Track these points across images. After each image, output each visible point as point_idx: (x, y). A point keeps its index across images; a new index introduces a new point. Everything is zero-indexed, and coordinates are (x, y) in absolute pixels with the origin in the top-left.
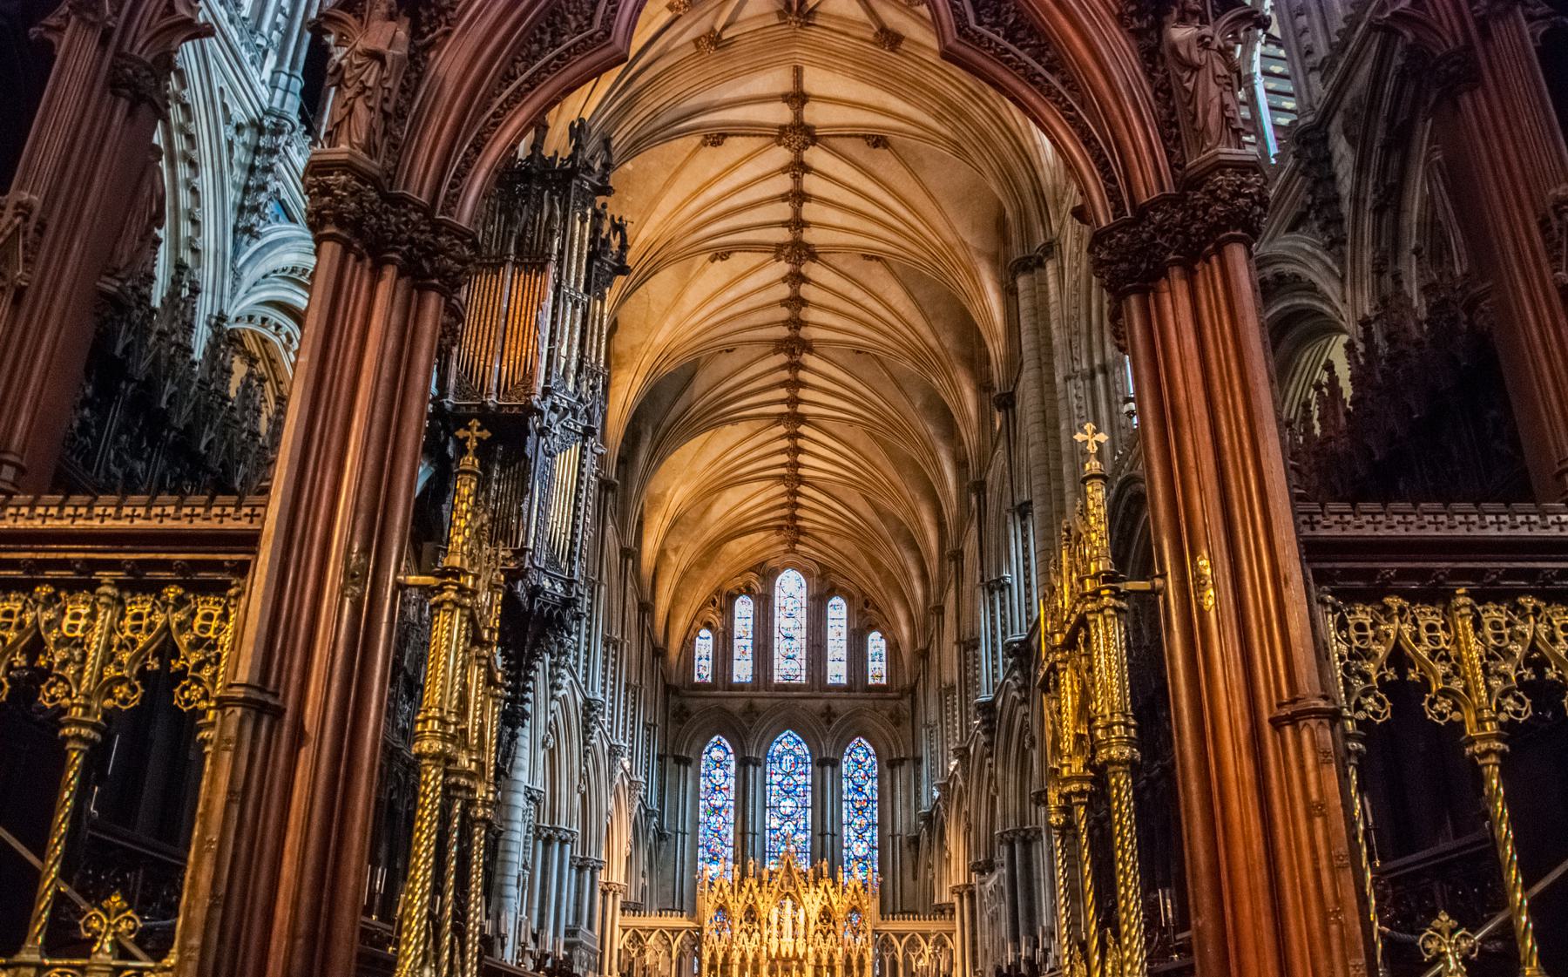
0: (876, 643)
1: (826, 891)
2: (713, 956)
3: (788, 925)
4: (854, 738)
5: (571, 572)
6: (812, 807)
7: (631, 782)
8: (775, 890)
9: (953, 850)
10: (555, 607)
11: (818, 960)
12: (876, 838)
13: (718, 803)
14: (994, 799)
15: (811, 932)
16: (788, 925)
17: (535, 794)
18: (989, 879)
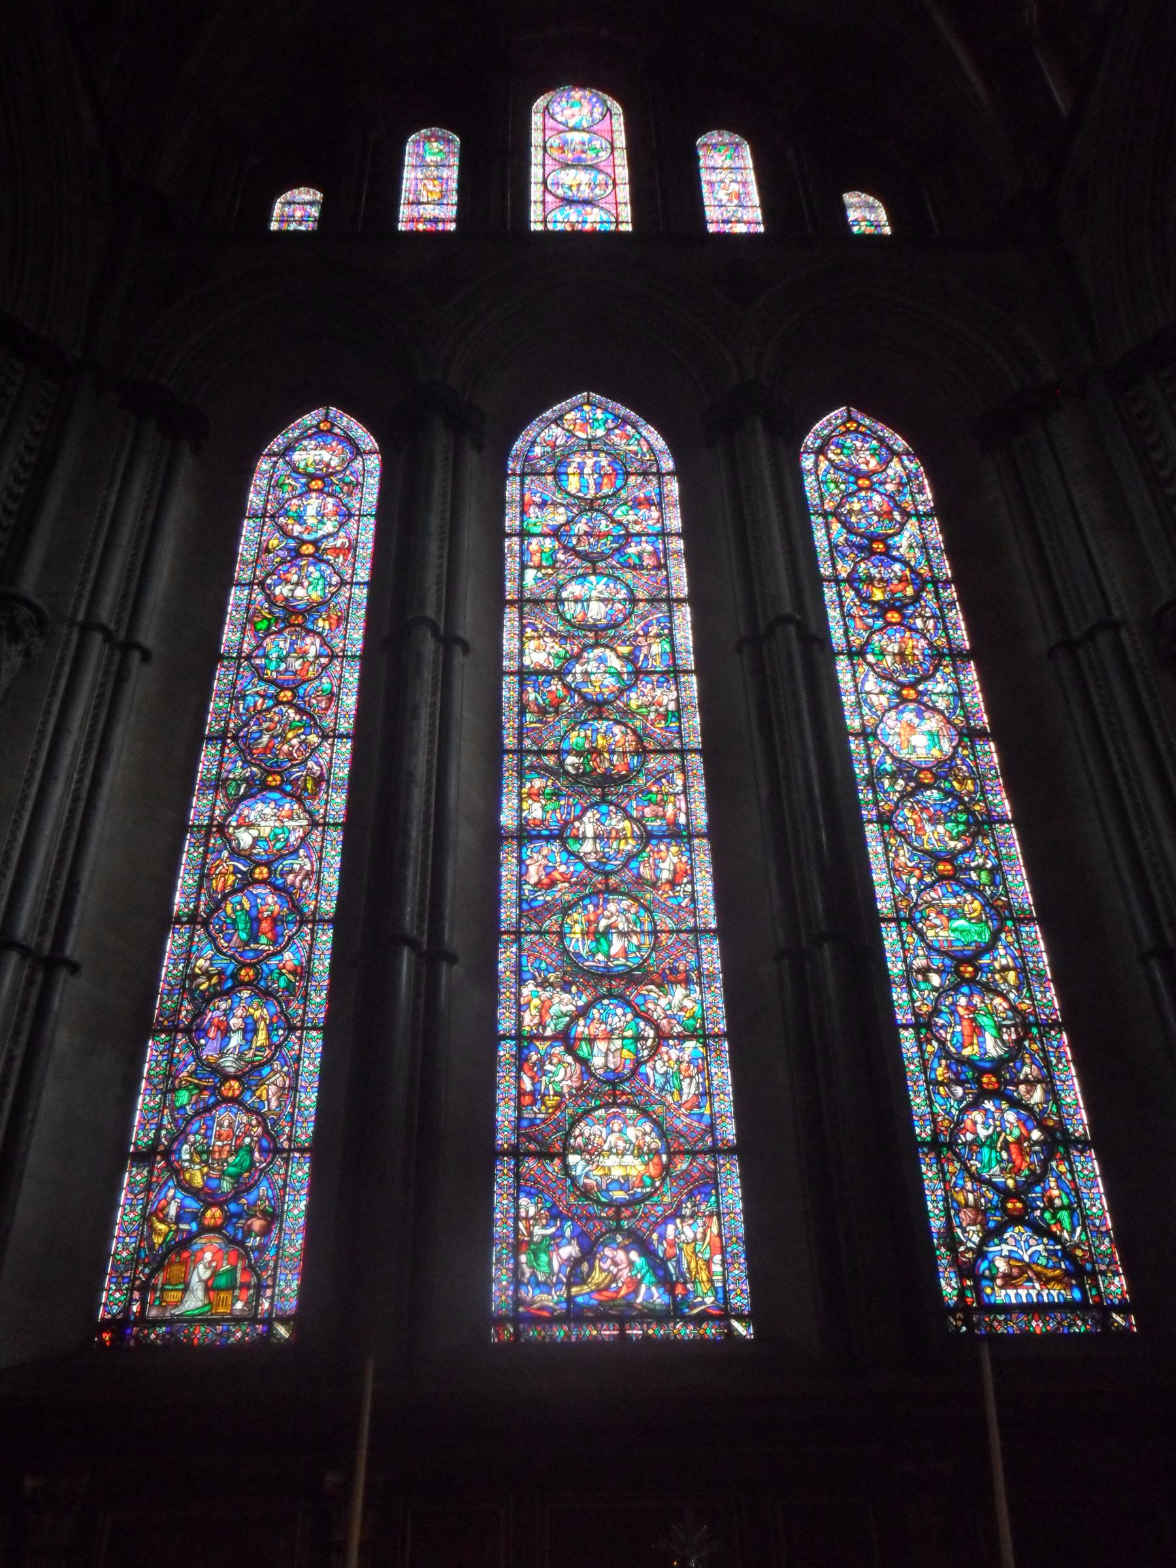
12: (976, 699)
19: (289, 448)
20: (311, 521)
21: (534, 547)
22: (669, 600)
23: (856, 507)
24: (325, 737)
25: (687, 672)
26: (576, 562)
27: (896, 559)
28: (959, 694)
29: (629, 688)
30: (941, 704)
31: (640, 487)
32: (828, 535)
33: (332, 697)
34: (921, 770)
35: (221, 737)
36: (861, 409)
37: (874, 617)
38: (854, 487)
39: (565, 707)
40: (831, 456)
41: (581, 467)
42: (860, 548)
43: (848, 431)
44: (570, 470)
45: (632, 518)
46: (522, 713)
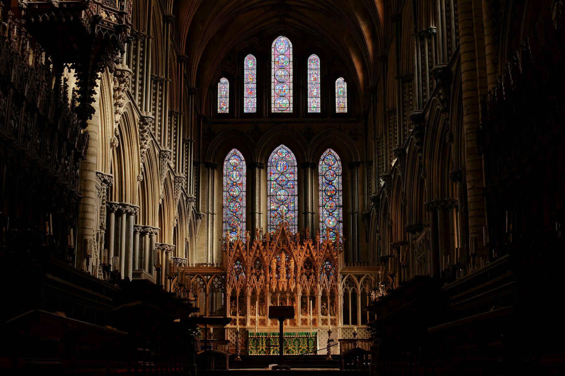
0: (341, 86)
1: (308, 247)
2: (234, 291)
3: (283, 270)
4: (325, 150)
5: (122, 7)
6: (298, 195)
7: (175, 177)
8: (274, 247)
9: (393, 219)
10: (111, 32)
11: (304, 293)
12: (341, 215)
13: (236, 194)
14: (422, 181)
15: (299, 275)
16: (283, 270)
17: (106, 178)
18: (419, 236)
19: (229, 159)
20: (235, 177)
21: (272, 183)
22: (294, 195)
23: (328, 174)
24: (241, 222)
25: (296, 210)
26: (279, 187)
27: (333, 186)
28: (339, 214)
29: (287, 213)
30: (335, 216)
31: (291, 169)
32: (322, 180)
33: (241, 215)
34: (330, 228)
35: (226, 222)
36: (332, 149)
37: (328, 199)
38: (328, 169)
39: (277, 217)
40: (325, 161)
41: (280, 165)
42: (327, 183)
43: (329, 154)
44: (279, 165)
45: (289, 177)
46: (270, 218)
